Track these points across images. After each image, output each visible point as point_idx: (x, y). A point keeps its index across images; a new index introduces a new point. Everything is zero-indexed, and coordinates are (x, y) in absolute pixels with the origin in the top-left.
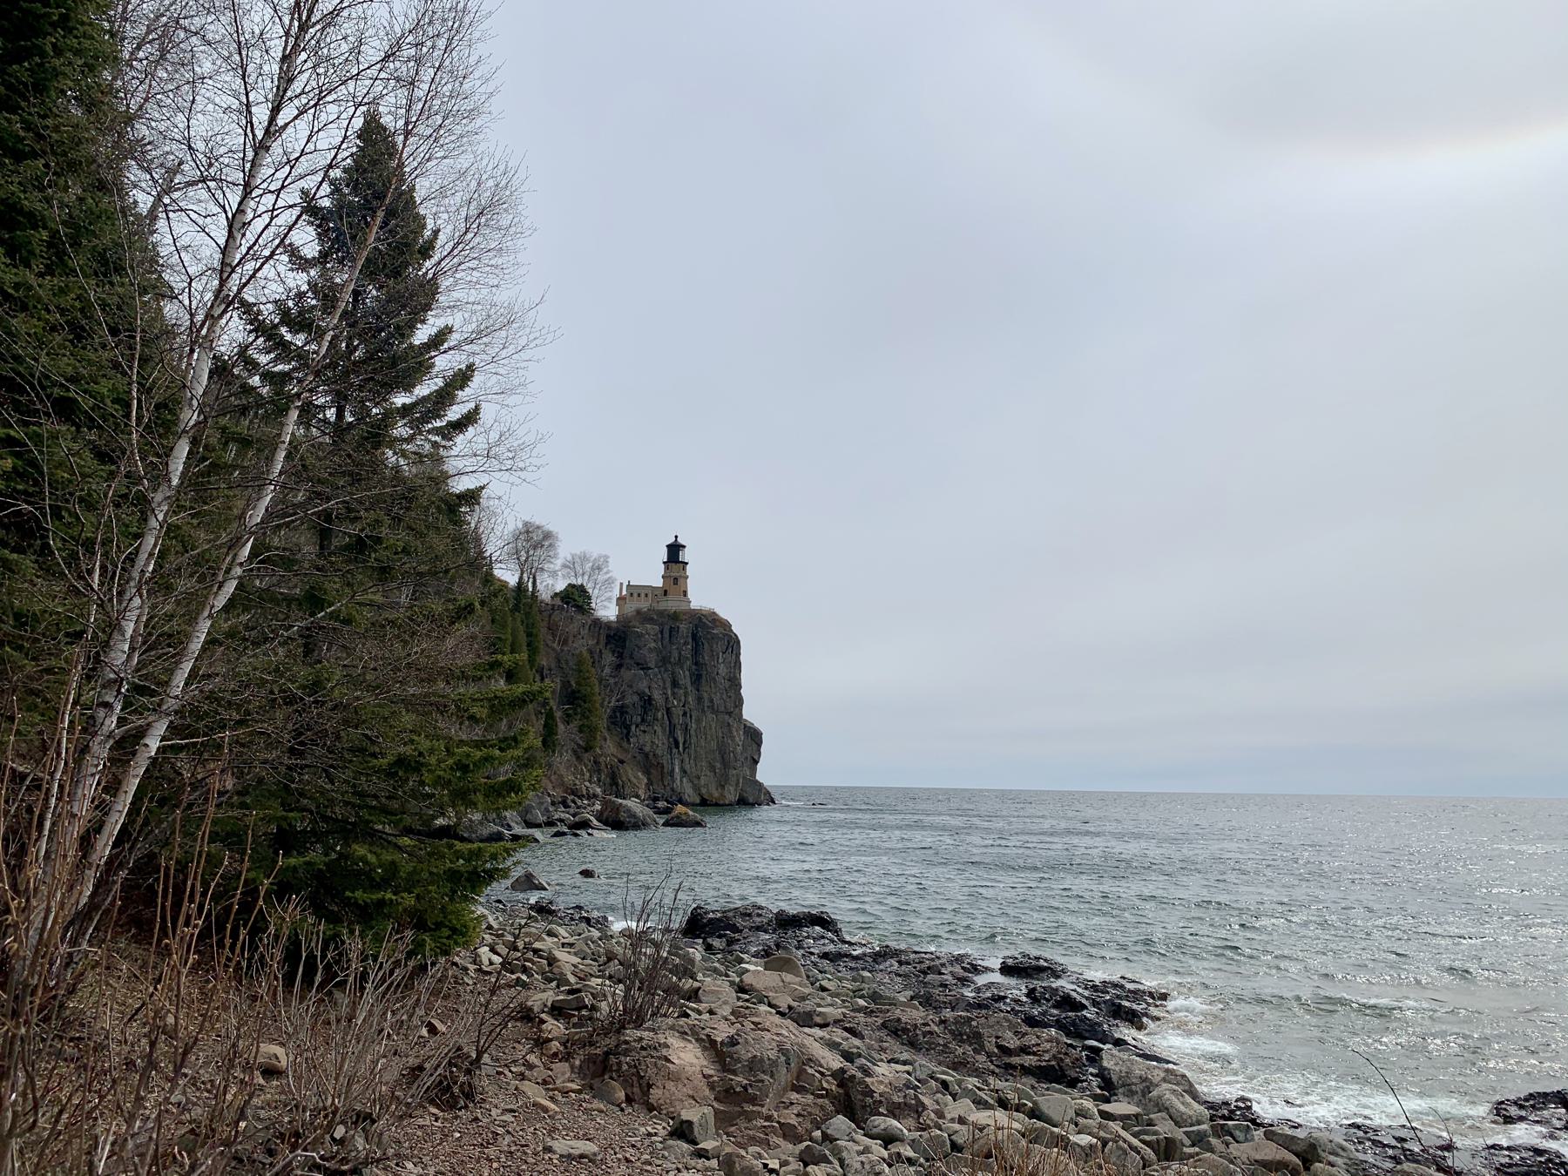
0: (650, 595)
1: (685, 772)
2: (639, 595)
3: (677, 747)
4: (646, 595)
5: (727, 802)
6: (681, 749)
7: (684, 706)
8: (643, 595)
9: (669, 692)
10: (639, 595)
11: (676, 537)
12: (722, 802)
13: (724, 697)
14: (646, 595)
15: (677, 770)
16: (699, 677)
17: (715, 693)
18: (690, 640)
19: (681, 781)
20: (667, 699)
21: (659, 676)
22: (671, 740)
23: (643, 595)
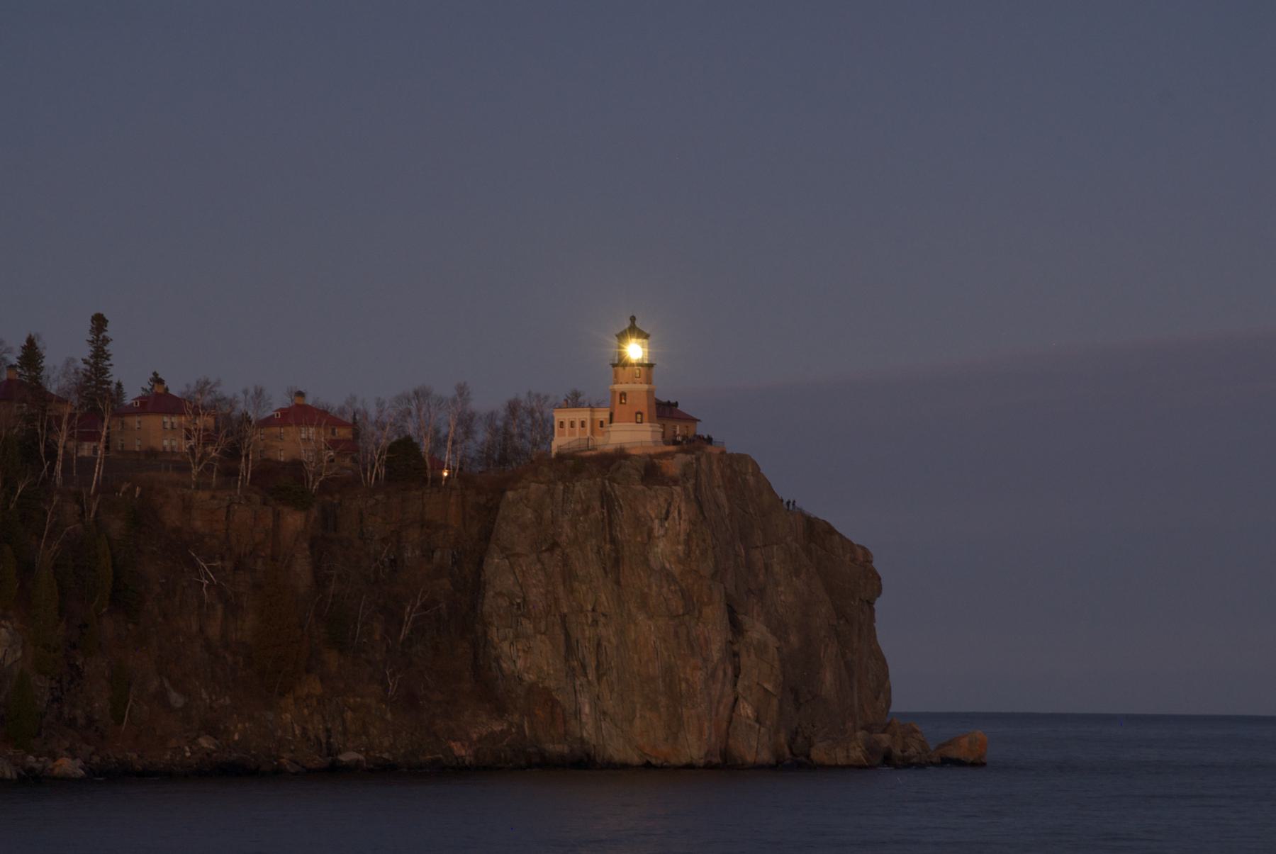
0: (588, 425)
1: (605, 713)
2: (572, 424)
3: (586, 675)
4: (583, 424)
5: (684, 760)
6: (592, 676)
7: (593, 610)
8: (578, 425)
9: (561, 588)
10: (572, 424)
11: (633, 319)
12: (673, 761)
13: (665, 590)
14: (583, 424)
15: (587, 709)
16: (617, 562)
17: (649, 586)
18: (597, 504)
19: (598, 728)
20: (556, 600)
21: (539, 566)
22: (575, 663)
23: (578, 425)
